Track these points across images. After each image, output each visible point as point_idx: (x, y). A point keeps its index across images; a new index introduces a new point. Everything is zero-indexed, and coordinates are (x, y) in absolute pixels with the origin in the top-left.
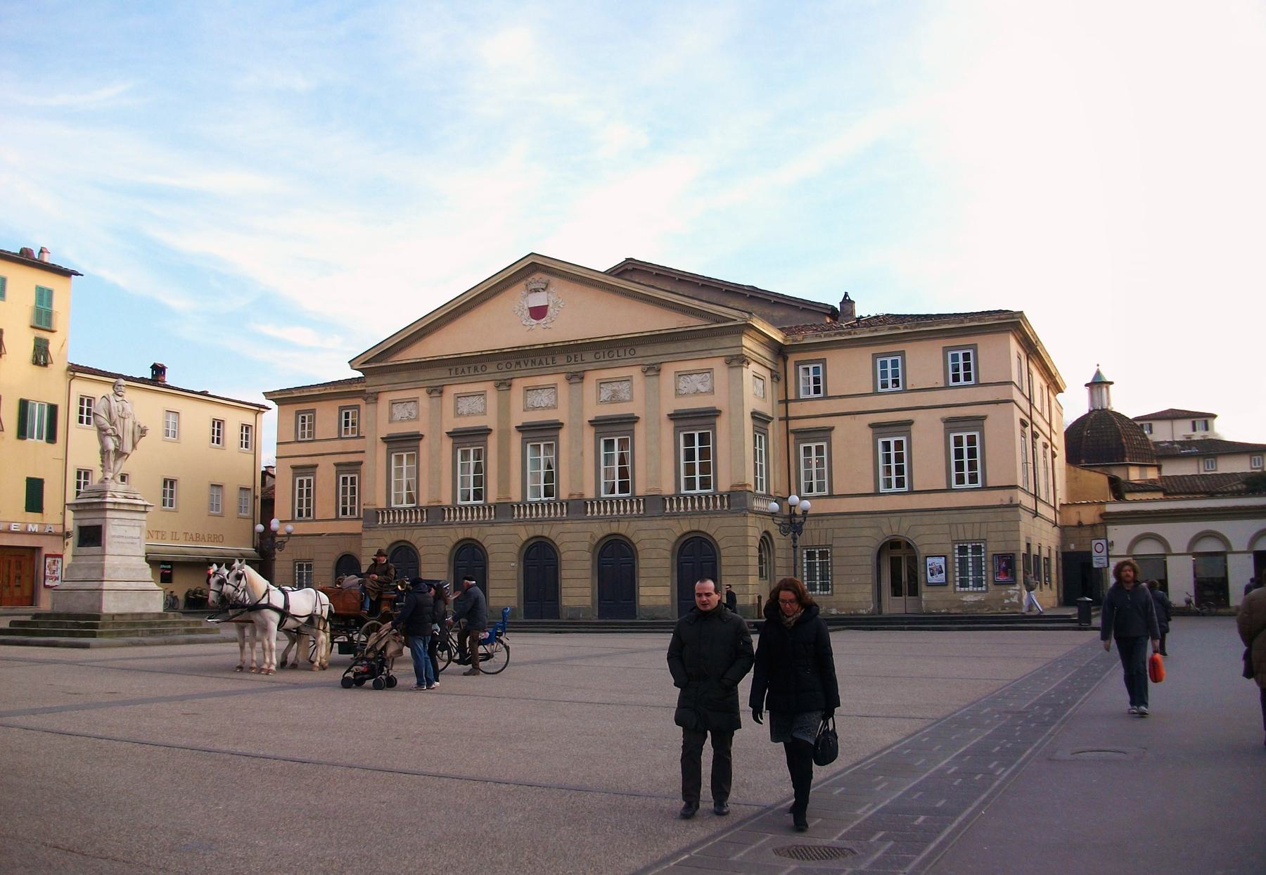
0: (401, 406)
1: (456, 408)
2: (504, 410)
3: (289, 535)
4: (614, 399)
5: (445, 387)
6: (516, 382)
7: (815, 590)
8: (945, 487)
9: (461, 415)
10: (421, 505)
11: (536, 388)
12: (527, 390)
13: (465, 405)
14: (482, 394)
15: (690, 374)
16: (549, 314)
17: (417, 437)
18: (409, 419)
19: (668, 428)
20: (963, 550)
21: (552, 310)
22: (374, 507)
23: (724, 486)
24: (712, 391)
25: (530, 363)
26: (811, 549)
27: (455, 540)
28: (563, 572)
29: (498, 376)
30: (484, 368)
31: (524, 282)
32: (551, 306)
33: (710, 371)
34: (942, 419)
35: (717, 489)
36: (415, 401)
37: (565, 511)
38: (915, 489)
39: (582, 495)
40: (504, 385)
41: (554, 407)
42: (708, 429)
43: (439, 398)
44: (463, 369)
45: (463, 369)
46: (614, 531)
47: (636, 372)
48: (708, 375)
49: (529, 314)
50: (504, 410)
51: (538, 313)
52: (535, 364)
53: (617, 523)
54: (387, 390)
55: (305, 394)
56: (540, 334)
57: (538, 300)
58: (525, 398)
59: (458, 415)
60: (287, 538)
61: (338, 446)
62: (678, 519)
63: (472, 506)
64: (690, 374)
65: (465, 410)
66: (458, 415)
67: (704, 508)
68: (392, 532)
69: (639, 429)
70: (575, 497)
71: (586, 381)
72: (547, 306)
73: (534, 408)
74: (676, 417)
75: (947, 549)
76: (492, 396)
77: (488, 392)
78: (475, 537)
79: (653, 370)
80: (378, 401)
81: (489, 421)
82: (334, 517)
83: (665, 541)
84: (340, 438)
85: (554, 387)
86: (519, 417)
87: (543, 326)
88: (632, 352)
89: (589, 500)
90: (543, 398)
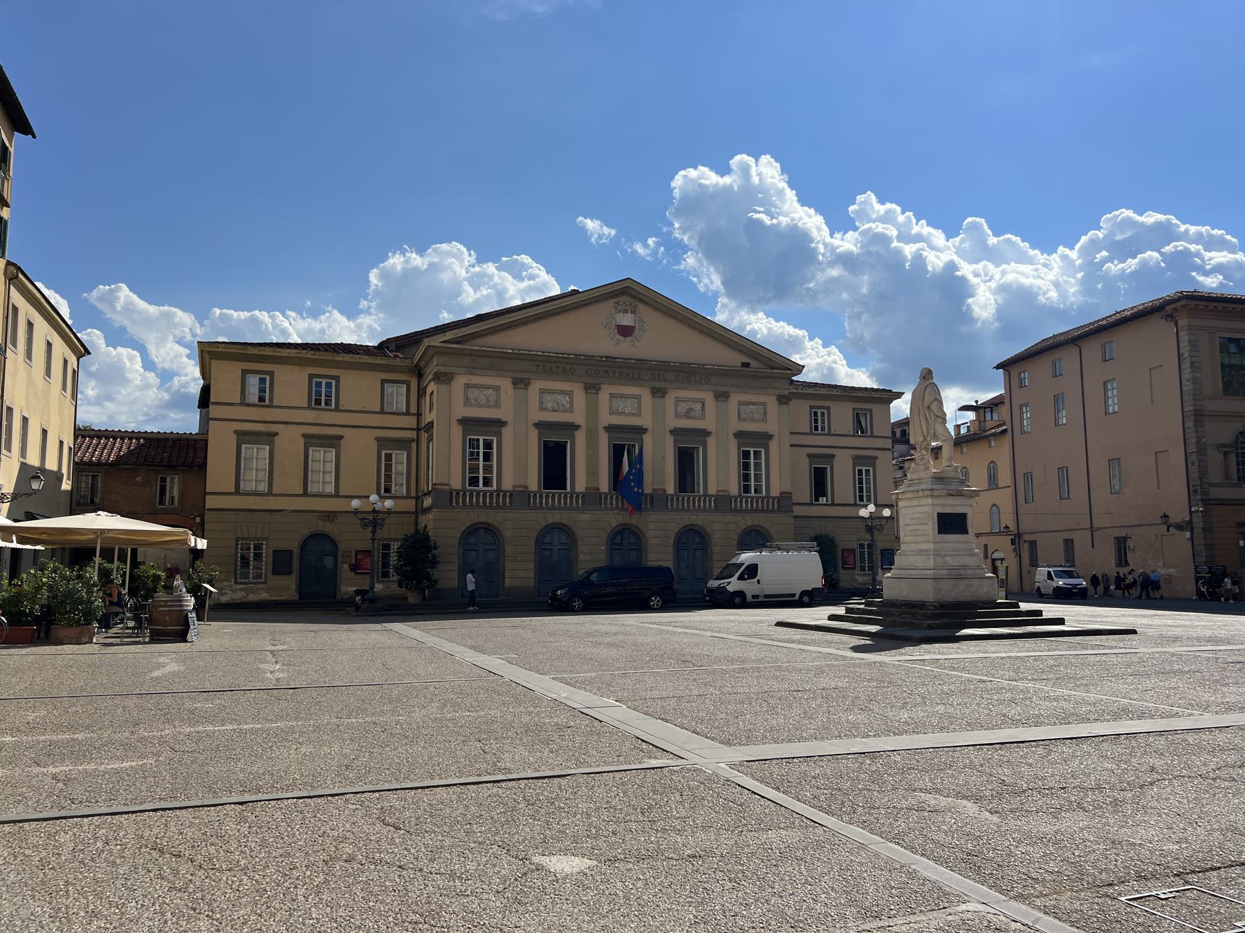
0: (476, 391)
1: (541, 403)
2: (592, 410)
3: (389, 512)
4: (688, 415)
5: (531, 380)
6: (604, 387)
7: (865, 570)
8: (853, 503)
9: (545, 409)
10: (577, 491)
11: (622, 396)
12: (612, 396)
13: (550, 401)
14: (570, 394)
15: (748, 404)
16: (635, 334)
17: (500, 423)
18: (488, 406)
19: (733, 444)
20: (862, 546)
21: (637, 330)
22: (447, 487)
23: (775, 492)
24: (764, 420)
25: (617, 375)
26: (258, 540)
27: (544, 523)
28: (649, 555)
29: (587, 380)
30: (573, 370)
31: (616, 300)
32: (637, 325)
33: (764, 404)
34: (852, 456)
35: (769, 493)
36: (497, 389)
37: (580, 502)
38: (836, 502)
39: (665, 490)
40: (592, 389)
41: (638, 414)
42: (761, 448)
43: (525, 391)
44: (551, 367)
45: (551, 367)
46: (693, 522)
47: (708, 397)
48: (762, 407)
49: (616, 331)
50: (592, 410)
51: (625, 331)
52: (622, 375)
53: (695, 517)
54: (462, 372)
55: (265, 353)
56: (625, 349)
57: (627, 320)
58: (611, 403)
59: (542, 408)
60: (387, 515)
61: (310, 416)
62: (743, 516)
63: (752, 498)
64: (748, 404)
65: (550, 405)
66: (542, 409)
67: (538, 504)
68: (472, 514)
69: (507, 432)
70: (661, 492)
71: (667, 396)
72: (634, 326)
73: (619, 414)
74: (739, 435)
75: (855, 546)
76: (580, 397)
77: (574, 393)
78: (564, 522)
79: (722, 396)
80: (666, 396)
81: (578, 417)
82: (302, 493)
83: (733, 533)
84: (309, 407)
85: (638, 397)
86: (606, 419)
87: (629, 343)
88: (707, 380)
89: (532, 492)
90: (629, 406)
